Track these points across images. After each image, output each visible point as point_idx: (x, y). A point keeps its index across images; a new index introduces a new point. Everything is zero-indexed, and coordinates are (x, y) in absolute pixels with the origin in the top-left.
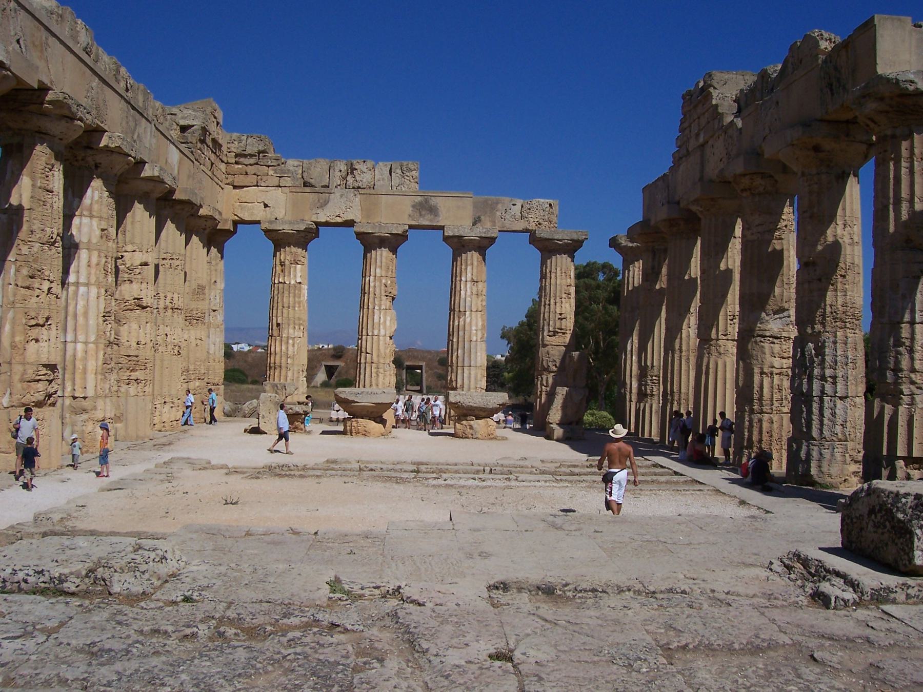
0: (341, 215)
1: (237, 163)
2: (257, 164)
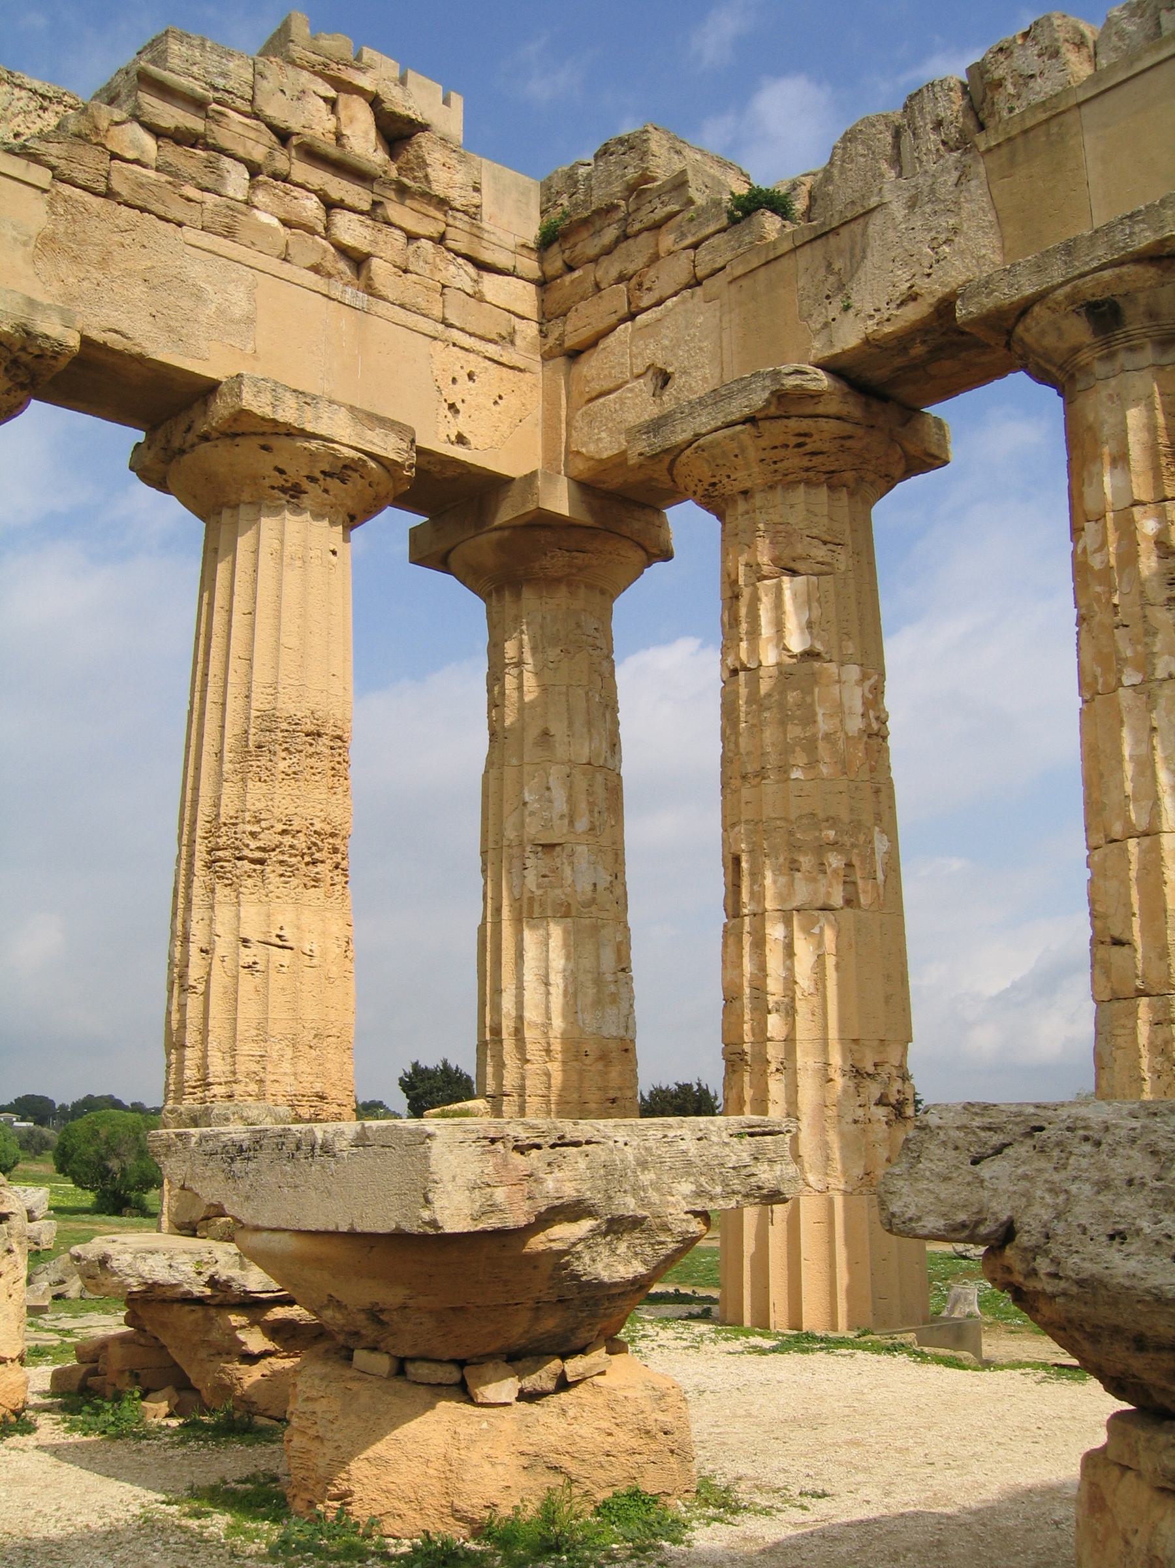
0: (922, 284)
1: (570, 269)
2: (625, 237)
